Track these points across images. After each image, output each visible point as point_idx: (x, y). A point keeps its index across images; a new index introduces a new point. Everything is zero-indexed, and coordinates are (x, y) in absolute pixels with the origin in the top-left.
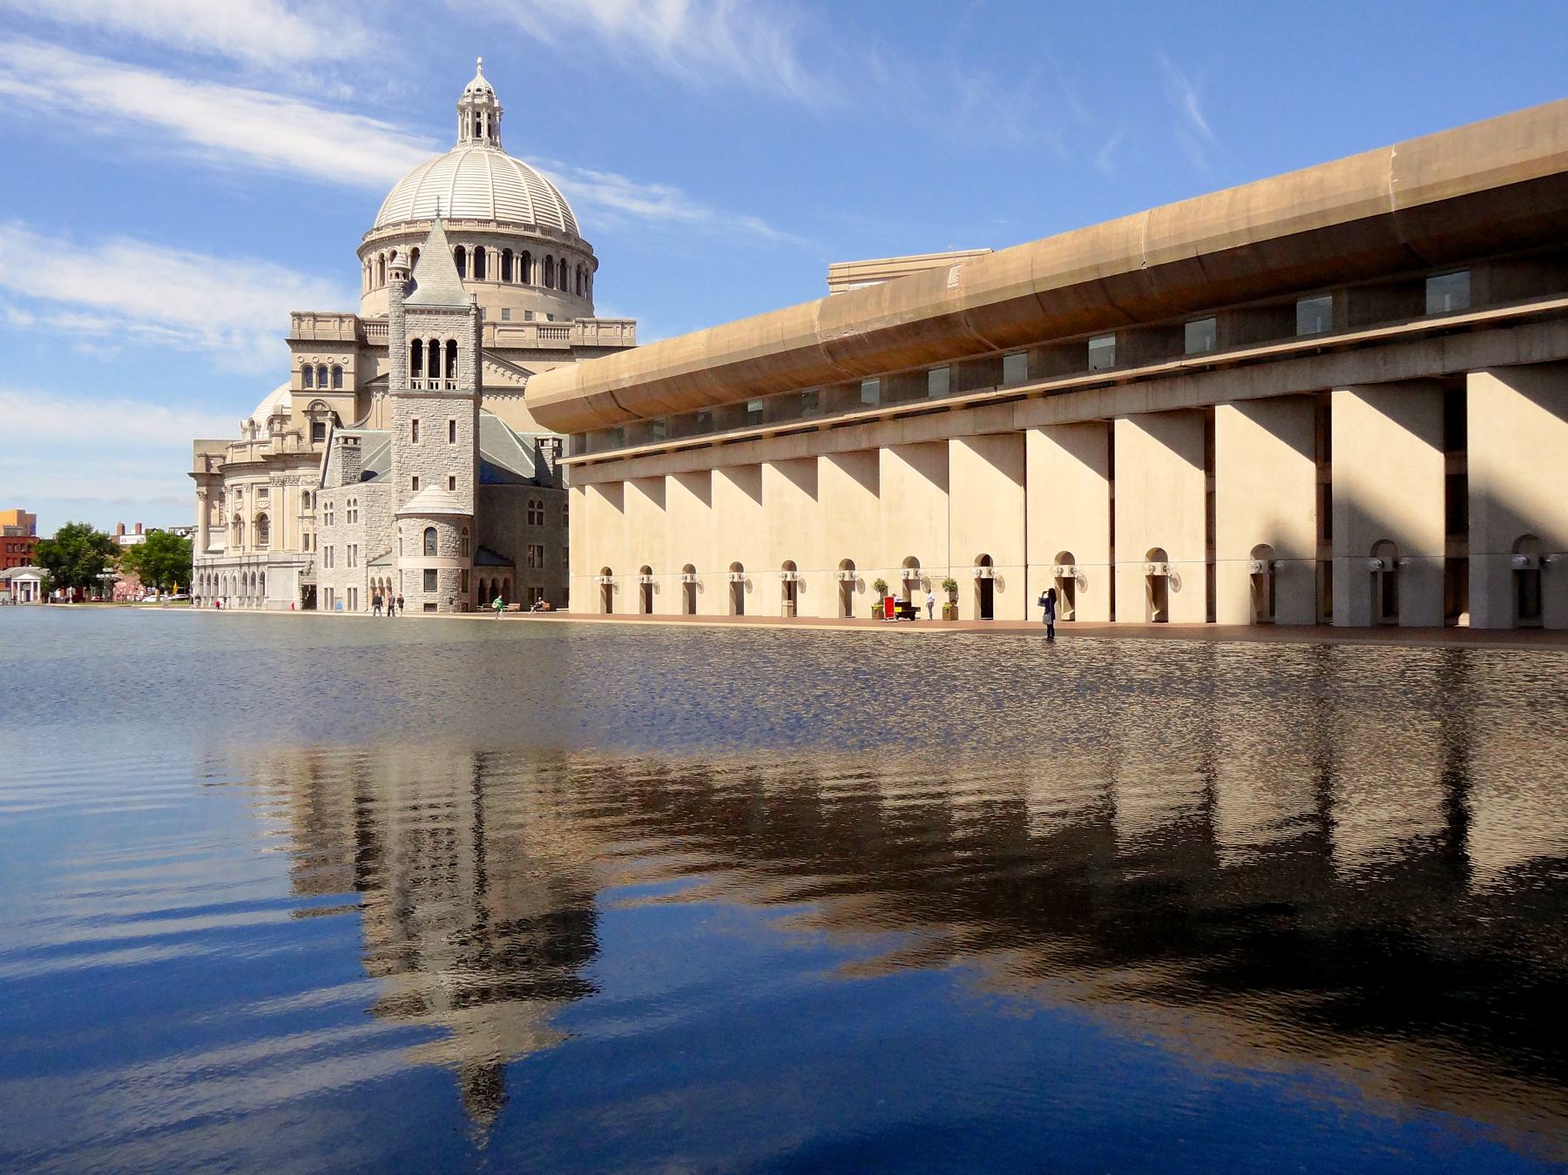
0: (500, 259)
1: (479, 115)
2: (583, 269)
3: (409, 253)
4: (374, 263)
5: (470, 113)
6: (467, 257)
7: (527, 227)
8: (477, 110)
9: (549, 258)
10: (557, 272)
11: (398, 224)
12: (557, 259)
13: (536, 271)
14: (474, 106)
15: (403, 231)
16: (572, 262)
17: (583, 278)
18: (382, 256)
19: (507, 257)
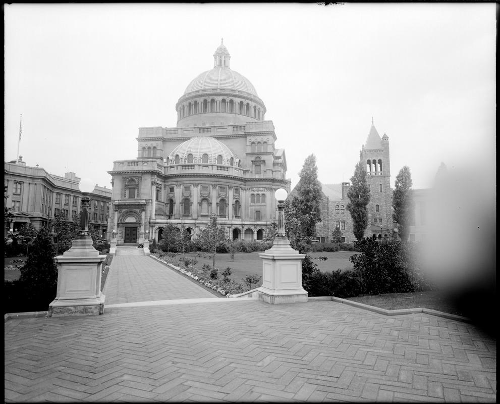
2: (257, 108)
3: (188, 104)
8: (220, 55)
10: (245, 107)
13: (237, 107)
14: (219, 54)
16: (252, 104)
17: (257, 111)
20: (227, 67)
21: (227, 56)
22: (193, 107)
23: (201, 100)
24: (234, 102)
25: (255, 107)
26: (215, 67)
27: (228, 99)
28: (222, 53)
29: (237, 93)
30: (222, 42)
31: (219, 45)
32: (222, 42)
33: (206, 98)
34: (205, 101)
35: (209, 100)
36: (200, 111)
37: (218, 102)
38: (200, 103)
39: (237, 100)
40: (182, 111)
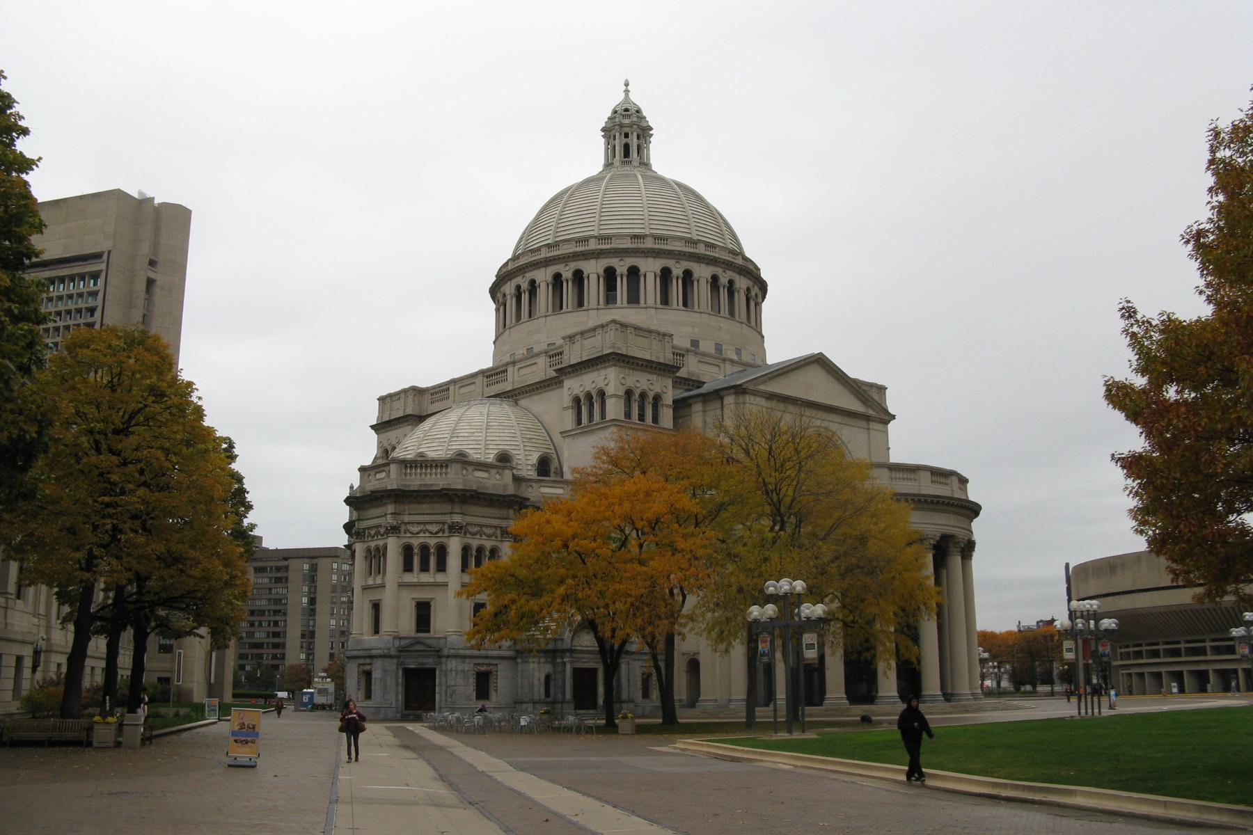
0: (658, 279)
1: (626, 136)
2: (753, 294)
3: (550, 279)
4: (508, 297)
5: (617, 135)
6: (619, 280)
7: (690, 242)
9: (715, 279)
11: (539, 249)
12: (724, 280)
13: (702, 291)
14: (621, 126)
15: (543, 256)
16: (742, 283)
17: (752, 304)
18: (518, 288)
19: (666, 274)
20: (645, 165)
21: (644, 132)
22: (569, 291)
23: (593, 269)
24: (696, 275)
25: (748, 289)
26: (608, 165)
27: (677, 270)
28: (631, 126)
29: (701, 249)
30: (627, 92)
31: (615, 99)
32: (627, 92)
33: (613, 262)
34: (610, 274)
35: (621, 267)
36: (593, 304)
37: (650, 278)
38: (593, 278)
39: (702, 273)
40: (525, 298)
